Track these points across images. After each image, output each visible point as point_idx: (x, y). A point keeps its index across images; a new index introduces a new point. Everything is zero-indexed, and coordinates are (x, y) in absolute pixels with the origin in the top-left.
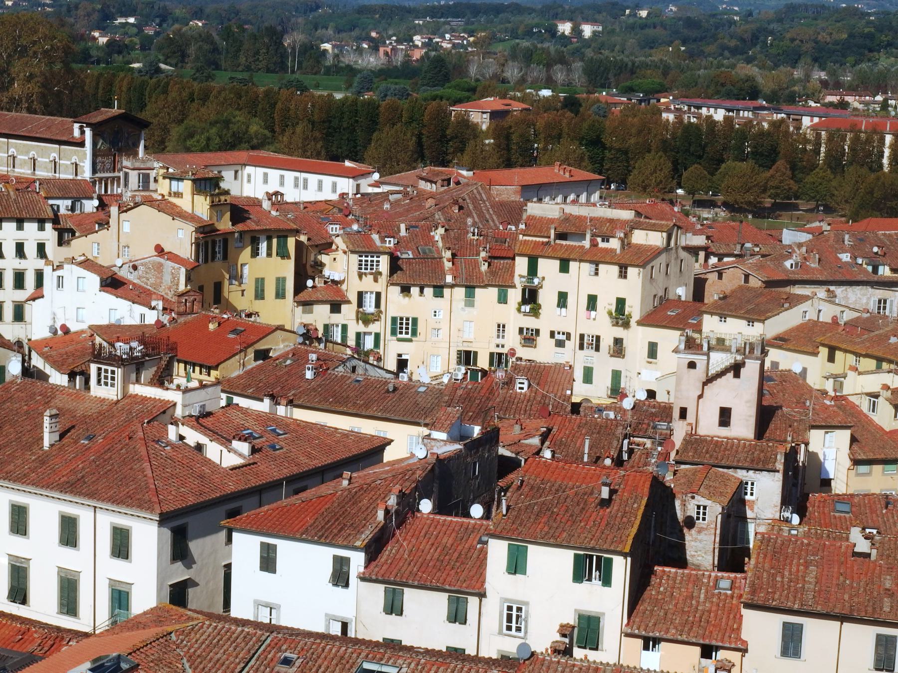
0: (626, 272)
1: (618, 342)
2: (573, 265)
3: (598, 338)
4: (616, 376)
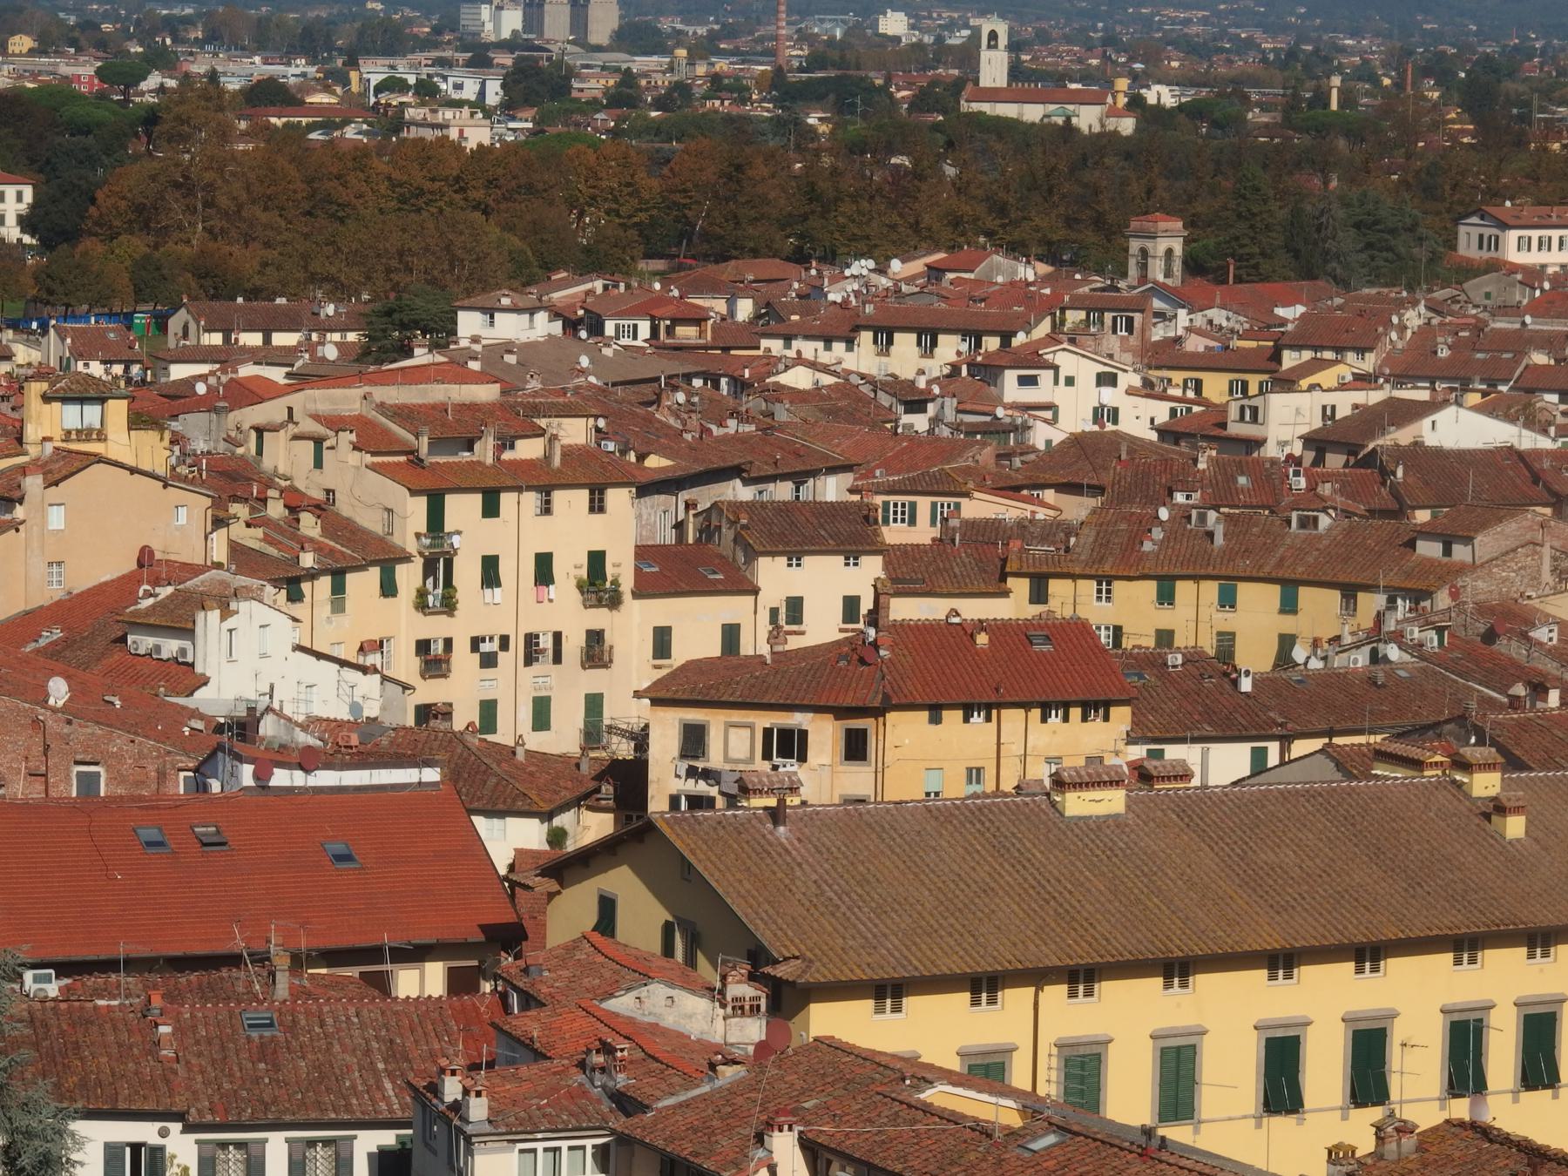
0: (601, 500)
1: (595, 638)
2: (507, 500)
3: (557, 637)
4: (594, 704)
